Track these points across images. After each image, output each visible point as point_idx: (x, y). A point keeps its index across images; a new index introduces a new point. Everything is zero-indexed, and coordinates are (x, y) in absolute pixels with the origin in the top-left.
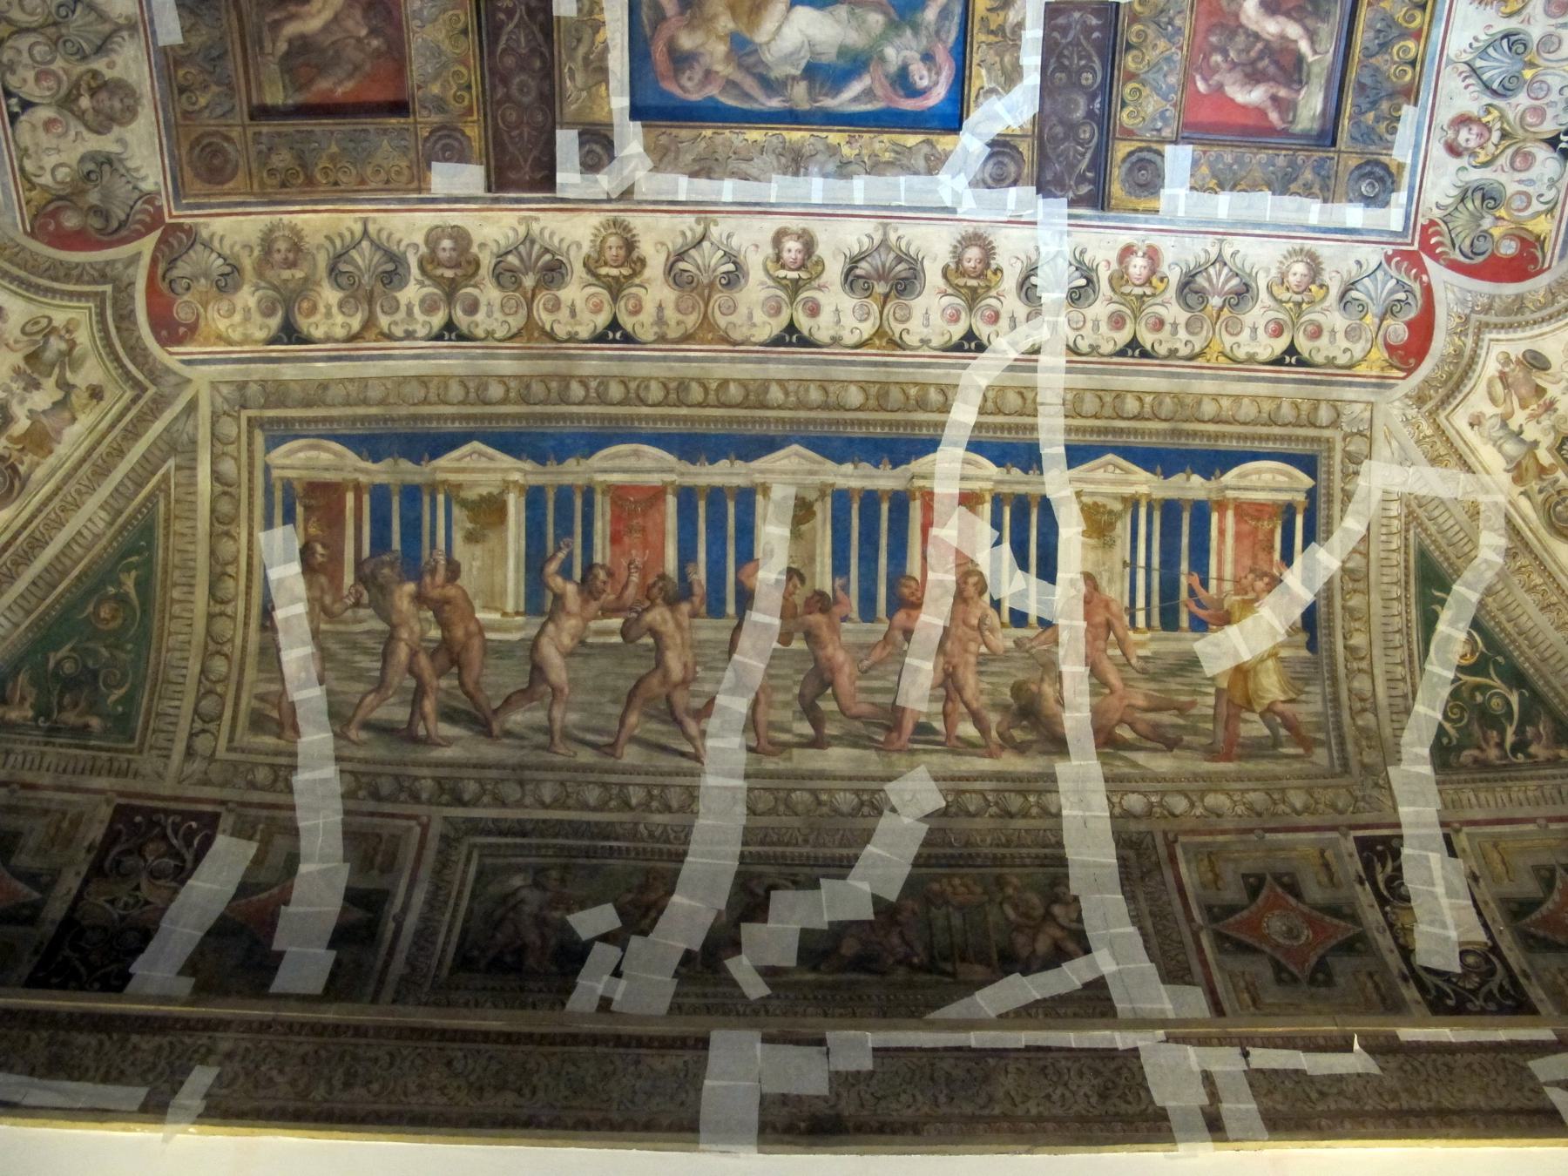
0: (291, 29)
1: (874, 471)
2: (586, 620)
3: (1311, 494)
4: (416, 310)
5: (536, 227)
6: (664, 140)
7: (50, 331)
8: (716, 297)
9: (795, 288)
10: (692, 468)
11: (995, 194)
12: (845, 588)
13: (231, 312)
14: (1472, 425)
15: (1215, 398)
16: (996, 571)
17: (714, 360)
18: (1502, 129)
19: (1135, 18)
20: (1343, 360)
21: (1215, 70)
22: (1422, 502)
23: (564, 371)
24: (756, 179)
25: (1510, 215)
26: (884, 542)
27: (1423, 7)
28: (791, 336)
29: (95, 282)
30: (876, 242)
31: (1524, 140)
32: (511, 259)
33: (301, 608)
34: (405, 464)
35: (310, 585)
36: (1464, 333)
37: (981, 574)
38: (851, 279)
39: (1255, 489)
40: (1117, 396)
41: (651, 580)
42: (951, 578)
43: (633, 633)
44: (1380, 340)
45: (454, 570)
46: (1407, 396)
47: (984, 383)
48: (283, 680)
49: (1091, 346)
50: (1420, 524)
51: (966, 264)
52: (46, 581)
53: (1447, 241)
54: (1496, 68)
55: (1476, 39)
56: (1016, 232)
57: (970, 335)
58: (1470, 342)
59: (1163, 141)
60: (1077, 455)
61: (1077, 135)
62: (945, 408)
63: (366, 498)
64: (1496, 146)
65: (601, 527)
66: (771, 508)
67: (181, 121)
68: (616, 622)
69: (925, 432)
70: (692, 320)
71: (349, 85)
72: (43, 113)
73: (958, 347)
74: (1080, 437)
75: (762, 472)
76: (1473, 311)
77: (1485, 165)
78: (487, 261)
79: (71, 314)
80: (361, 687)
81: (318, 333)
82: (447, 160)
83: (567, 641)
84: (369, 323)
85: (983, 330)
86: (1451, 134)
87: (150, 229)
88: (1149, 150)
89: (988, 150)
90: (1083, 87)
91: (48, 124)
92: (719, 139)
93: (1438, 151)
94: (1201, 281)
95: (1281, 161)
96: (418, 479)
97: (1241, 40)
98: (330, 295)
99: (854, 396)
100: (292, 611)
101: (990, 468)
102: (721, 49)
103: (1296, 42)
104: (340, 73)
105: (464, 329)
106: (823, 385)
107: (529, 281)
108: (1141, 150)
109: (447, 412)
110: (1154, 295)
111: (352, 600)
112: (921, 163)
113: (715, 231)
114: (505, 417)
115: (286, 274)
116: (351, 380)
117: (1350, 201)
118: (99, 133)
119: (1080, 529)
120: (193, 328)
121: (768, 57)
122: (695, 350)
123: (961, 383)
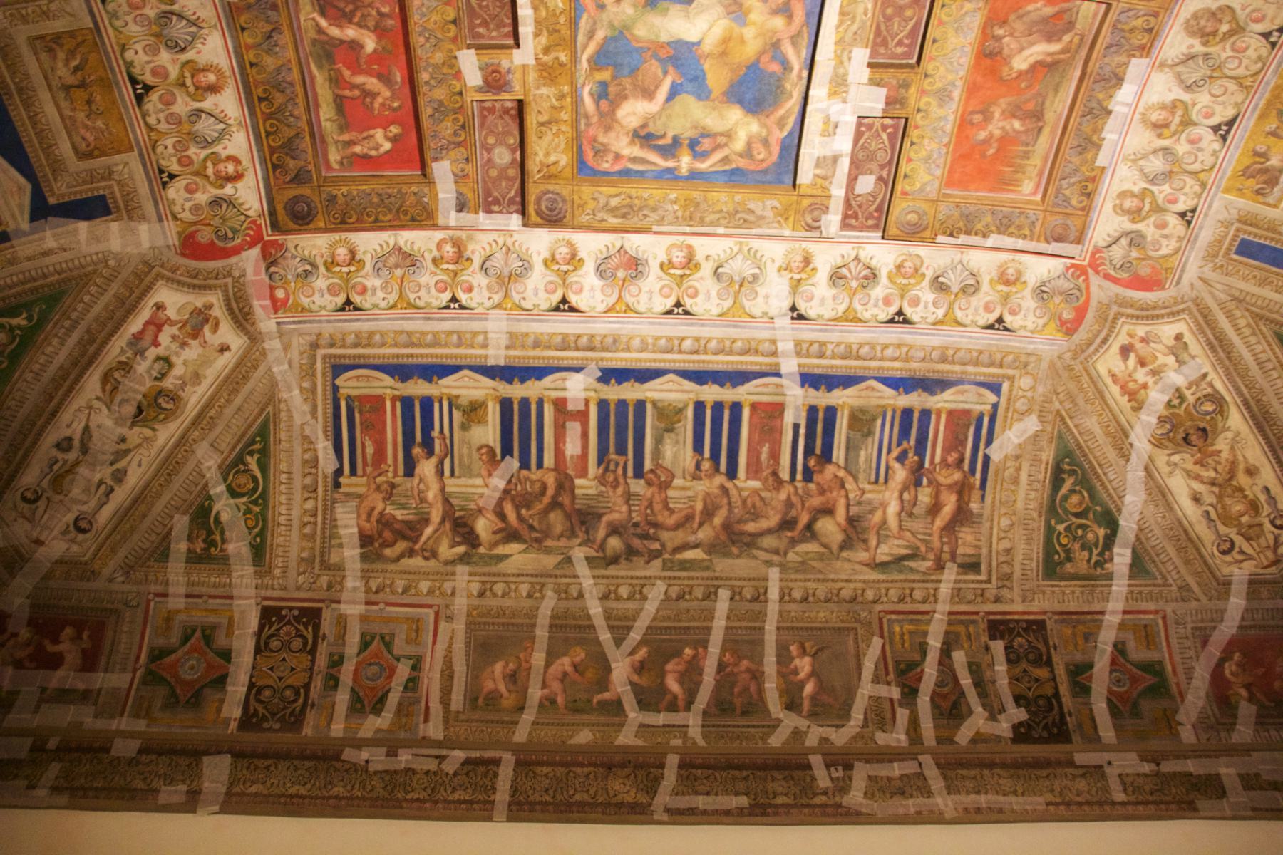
0: (1055, 47)
19: (454, 40)
27: (252, 65)
54: (179, 30)
67: (1162, 11)
97: (371, 24)
102: (753, 16)
104: (1034, 16)
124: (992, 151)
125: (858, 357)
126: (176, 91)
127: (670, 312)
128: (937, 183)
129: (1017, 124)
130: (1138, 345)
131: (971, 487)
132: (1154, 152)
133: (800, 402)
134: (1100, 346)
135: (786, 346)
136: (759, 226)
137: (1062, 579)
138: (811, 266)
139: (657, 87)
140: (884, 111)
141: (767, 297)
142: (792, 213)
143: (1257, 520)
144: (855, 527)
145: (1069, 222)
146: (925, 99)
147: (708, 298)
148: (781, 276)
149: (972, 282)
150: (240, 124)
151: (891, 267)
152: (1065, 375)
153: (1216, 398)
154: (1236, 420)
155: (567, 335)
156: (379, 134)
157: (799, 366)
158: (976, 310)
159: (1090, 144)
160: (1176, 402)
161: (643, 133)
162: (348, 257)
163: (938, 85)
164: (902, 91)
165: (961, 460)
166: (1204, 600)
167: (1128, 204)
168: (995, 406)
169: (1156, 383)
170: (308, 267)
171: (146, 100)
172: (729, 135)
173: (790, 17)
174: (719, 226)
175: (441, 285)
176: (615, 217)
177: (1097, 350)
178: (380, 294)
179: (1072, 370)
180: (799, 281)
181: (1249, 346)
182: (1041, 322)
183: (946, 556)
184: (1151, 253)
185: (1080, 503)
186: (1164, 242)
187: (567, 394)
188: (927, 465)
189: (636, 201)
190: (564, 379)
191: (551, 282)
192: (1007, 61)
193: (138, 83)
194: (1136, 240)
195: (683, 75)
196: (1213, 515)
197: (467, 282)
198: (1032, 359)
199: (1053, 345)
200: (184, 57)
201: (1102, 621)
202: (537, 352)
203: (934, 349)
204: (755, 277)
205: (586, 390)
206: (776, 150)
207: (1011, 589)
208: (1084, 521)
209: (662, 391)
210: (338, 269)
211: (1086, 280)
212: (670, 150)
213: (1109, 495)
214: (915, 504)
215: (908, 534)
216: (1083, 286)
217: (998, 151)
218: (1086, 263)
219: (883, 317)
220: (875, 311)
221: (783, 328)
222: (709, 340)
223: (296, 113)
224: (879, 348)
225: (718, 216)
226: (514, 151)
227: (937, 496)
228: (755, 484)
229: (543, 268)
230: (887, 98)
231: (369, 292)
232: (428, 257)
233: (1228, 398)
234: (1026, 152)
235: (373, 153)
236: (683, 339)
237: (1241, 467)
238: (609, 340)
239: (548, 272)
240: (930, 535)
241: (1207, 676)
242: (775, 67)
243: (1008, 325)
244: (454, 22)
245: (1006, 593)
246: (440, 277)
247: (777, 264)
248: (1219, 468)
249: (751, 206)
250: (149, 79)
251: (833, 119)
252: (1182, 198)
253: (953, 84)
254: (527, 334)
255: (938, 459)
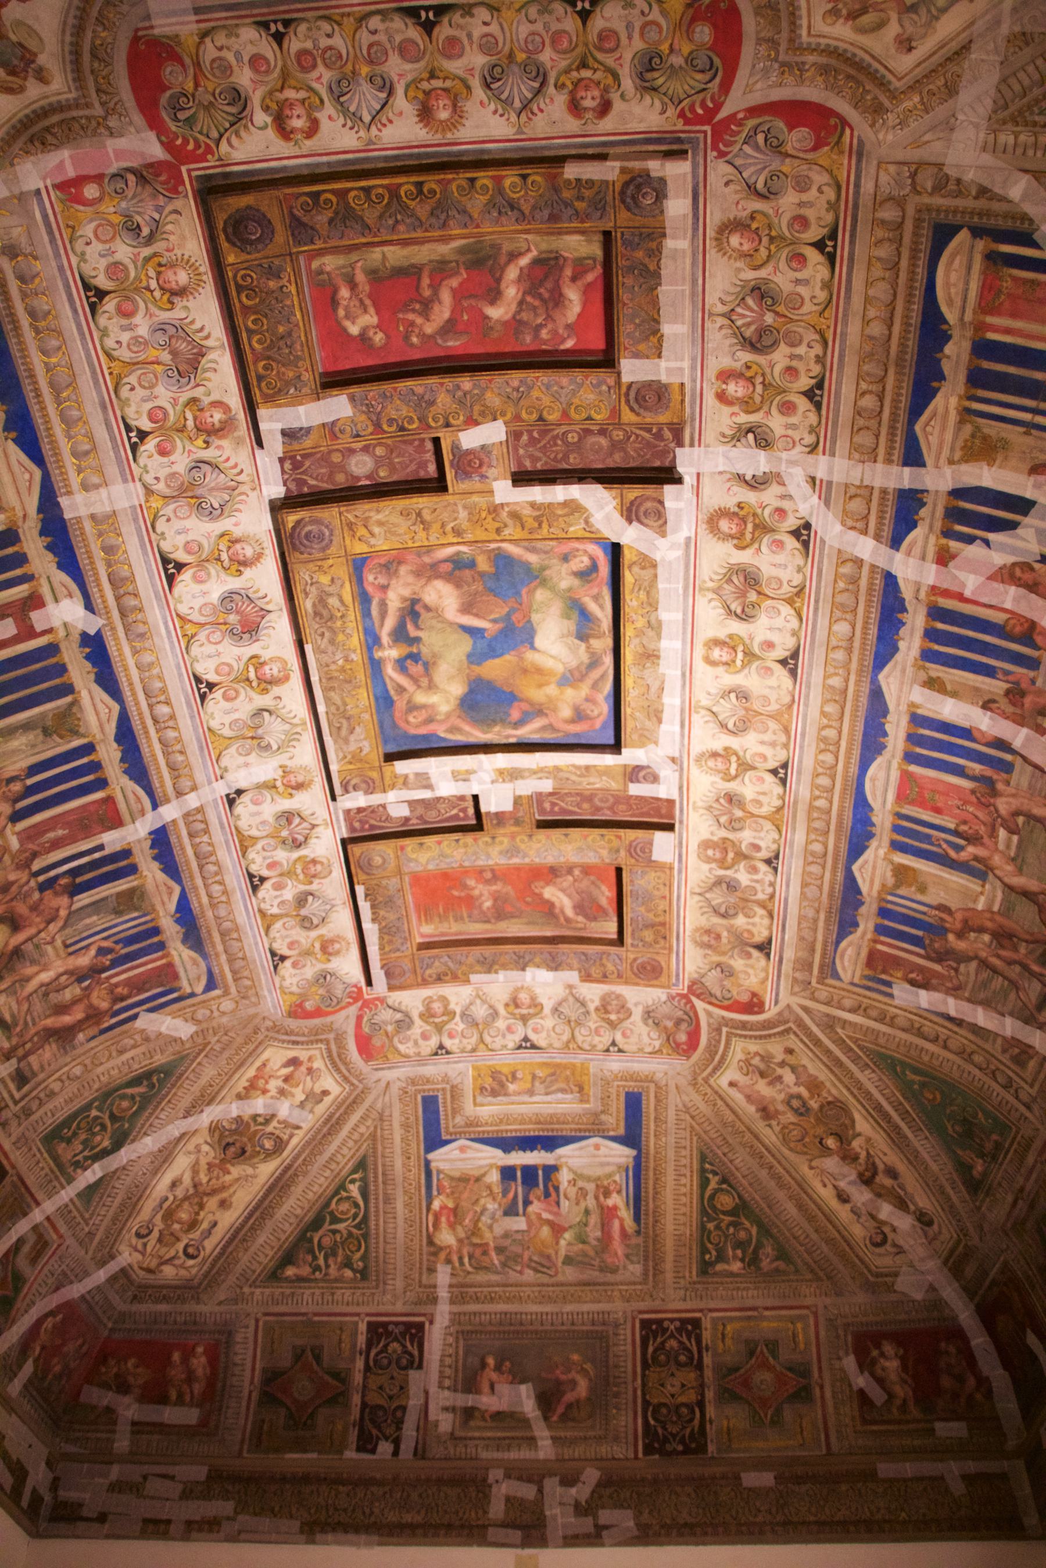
0: (570, 912)
1: (908, 626)
2: (997, 849)
3: (977, 232)
4: (755, 877)
5: (700, 804)
6: (635, 737)
7: (747, 1062)
8: (755, 707)
9: (750, 655)
10: (890, 748)
11: (671, 517)
12: (1007, 673)
13: (746, 973)
14: (910, 49)
15: (866, 322)
16: (1014, 551)
17: (805, 716)
18: (578, 69)
19: (517, 418)
20: (830, 194)
21: (554, 332)
22: (1001, 104)
23: (806, 807)
24: (663, 682)
25: (666, 38)
26: (971, 634)
27: (472, 180)
28: (790, 662)
29: (720, 1034)
30: (715, 596)
31: (586, 45)
32: (723, 819)
33: (951, 1001)
34: (863, 910)
35: (935, 989)
36: (801, 67)
37: (1014, 564)
38: (745, 616)
39: (966, 290)
40: (859, 414)
41: (975, 800)
42: (1013, 589)
43: (1013, 826)
44: (809, 156)
45: (942, 908)
46: (872, 126)
47: (838, 527)
48: (997, 1035)
49: (810, 433)
50: (1029, 107)
51: (734, 531)
52: (904, 1115)
53: (701, 96)
54: (519, 87)
55: (495, 112)
56: (706, 490)
57: (796, 533)
58: (811, 59)
59: (618, 382)
60: (913, 457)
61: (620, 441)
62: (859, 562)
63: (882, 938)
64: (595, 70)
65: (926, 816)
66: (929, 706)
68: (1002, 833)
69: (878, 581)
70: (772, 725)
71: (604, 888)
72: (619, 1038)
73: (806, 544)
74: (896, 452)
75: (898, 705)
76: (776, 60)
77: (616, 76)
78: (723, 833)
79: (738, 1049)
80: (1012, 996)
81: (765, 934)
82: (651, 851)
83: (1009, 868)
84: (762, 905)
85: (792, 522)
86: (589, 115)
87: (690, 1001)
88: (627, 394)
89: (635, 523)
90: (580, 439)
91: (624, 1035)
92: (633, 704)
93: (607, 124)
94: (748, 333)
95: (629, 281)
96: (874, 908)
97: (524, 316)
98: (740, 921)
99: (842, 628)
100: (952, 1006)
101: (917, 535)
102: (569, 692)
103: (521, 269)
104: (595, 892)
105: (772, 855)
106: (830, 648)
107: (739, 813)
108: (628, 402)
109: (830, 878)
110: (763, 375)
111: (953, 973)
112: (647, 574)
113: (705, 702)
114: (836, 847)
115: (724, 940)
116: (799, 923)
117: (662, 212)
118: (630, 1015)
119: (986, 467)
120: (754, 995)
121: (574, 663)
122: (796, 726)
123: (837, 545)
124: (456, 893)
125: (201, 867)
126: (422, 64)
127: (198, 680)
128: (420, 868)
129: (488, 904)
130: (303, 1069)
131: (98, 1023)
132: (491, 1007)
133: (131, 839)
134: (289, 1042)
135: (192, 801)
136: (335, 742)
137: (49, 1152)
138: (294, 792)
139: (477, 615)
140: (489, 813)
141: (247, 765)
142: (359, 765)
143: (180, 1235)
144: (11, 959)
145: (408, 975)
146: (506, 840)
147: (227, 713)
148: (275, 770)
149: (315, 921)
150: (370, 142)
151: (312, 856)
152: (249, 1030)
153: (280, 1144)
154: (267, 1170)
155: (134, 581)
156: (370, 319)
157: (174, 821)
158: (287, 936)
159: (489, 966)
160: (260, 1120)
161: (417, 608)
162: (174, 285)
163: (523, 846)
164: (512, 822)
165: (123, 999)
166: (90, 1253)
167: (437, 1006)
168: (192, 995)
169: (272, 1097)
170: (146, 231)
171: (410, 21)
172: (432, 687)
173: (572, 721)
174: (327, 706)
175: (161, 416)
176: (314, 605)
177: (283, 1041)
178: (125, 337)
179: (255, 1033)
180: (275, 787)
181: (344, 1143)
182: (294, 989)
183: (20, 1052)
184: (396, 1040)
185: (124, 1110)
186: (410, 1044)
187: (51, 607)
188: (104, 975)
189: (339, 623)
190: (70, 596)
191: (200, 547)
192: (548, 883)
193: (435, 16)
194: (404, 1023)
195: (495, 638)
196: (165, 1206)
197: (174, 447)
198: (253, 999)
199: (275, 1007)
200: (476, 83)
201: (32, 1210)
202: (99, 555)
203: (234, 921)
204: (268, 746)
205: (65, 625)
206: (423, 731)
207: (20, 1124)
208: (109, 1124)
209: (94, 705)
210: (152, 273)
211: (350, 1004)
212: (400, 635)
213: (143, 1125)
214: (58, 991)
215: (26, 1006)
216: (343, 1004)
217: (459, 898)
218: (366, 997)
219: (254, 869)
220: (259, 860)
221: (214, 791)
222: (175, 728)
223: (401, 228)
224: (218, 878)
225: (339, 702)
226: (368, 477)
227: (75, 1002)
228: (14, 843)
229: (218, 532)
230: (503, 813)
231: (124, 322)
232: (198, 392)
233: (285, 1154)
234: (462, 918)
235: (341, 313)
236: (168, 703)
237: (224, 1195)
238: (141, 628)
239: (212, 540)
240: (34, 1025)
241: (35, 1318)
242: (515, 715)
243: (280, 966)
244: (541, 419)
245: (14, 1123)
246: (171, 412)
247: (289, 763)
248: (214, 1181)
249: (358, 730)
250: (443, 31)
251: (472, 777)
252: (456, 1041)
253: (525, 856)
254: (119, 535)
255: (114, 980)
